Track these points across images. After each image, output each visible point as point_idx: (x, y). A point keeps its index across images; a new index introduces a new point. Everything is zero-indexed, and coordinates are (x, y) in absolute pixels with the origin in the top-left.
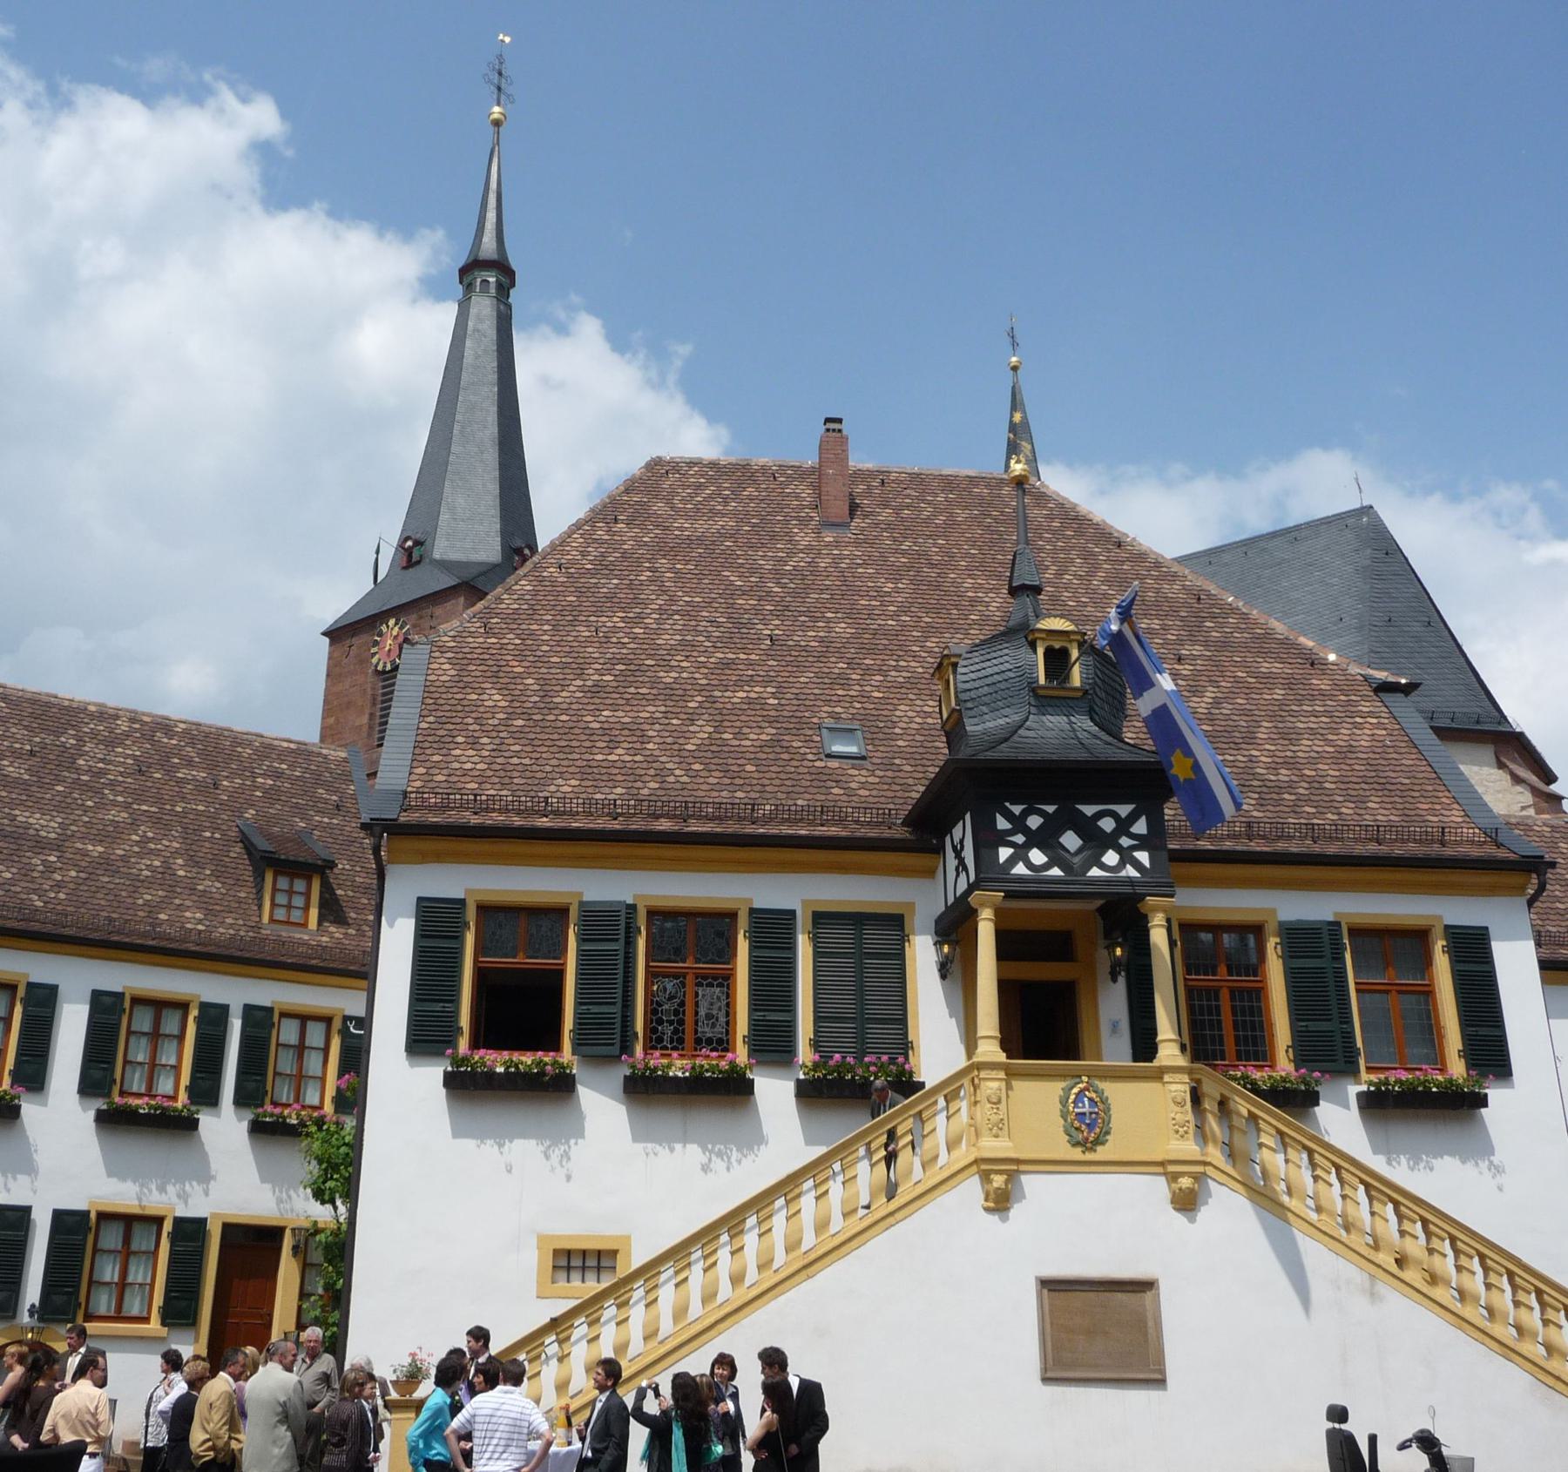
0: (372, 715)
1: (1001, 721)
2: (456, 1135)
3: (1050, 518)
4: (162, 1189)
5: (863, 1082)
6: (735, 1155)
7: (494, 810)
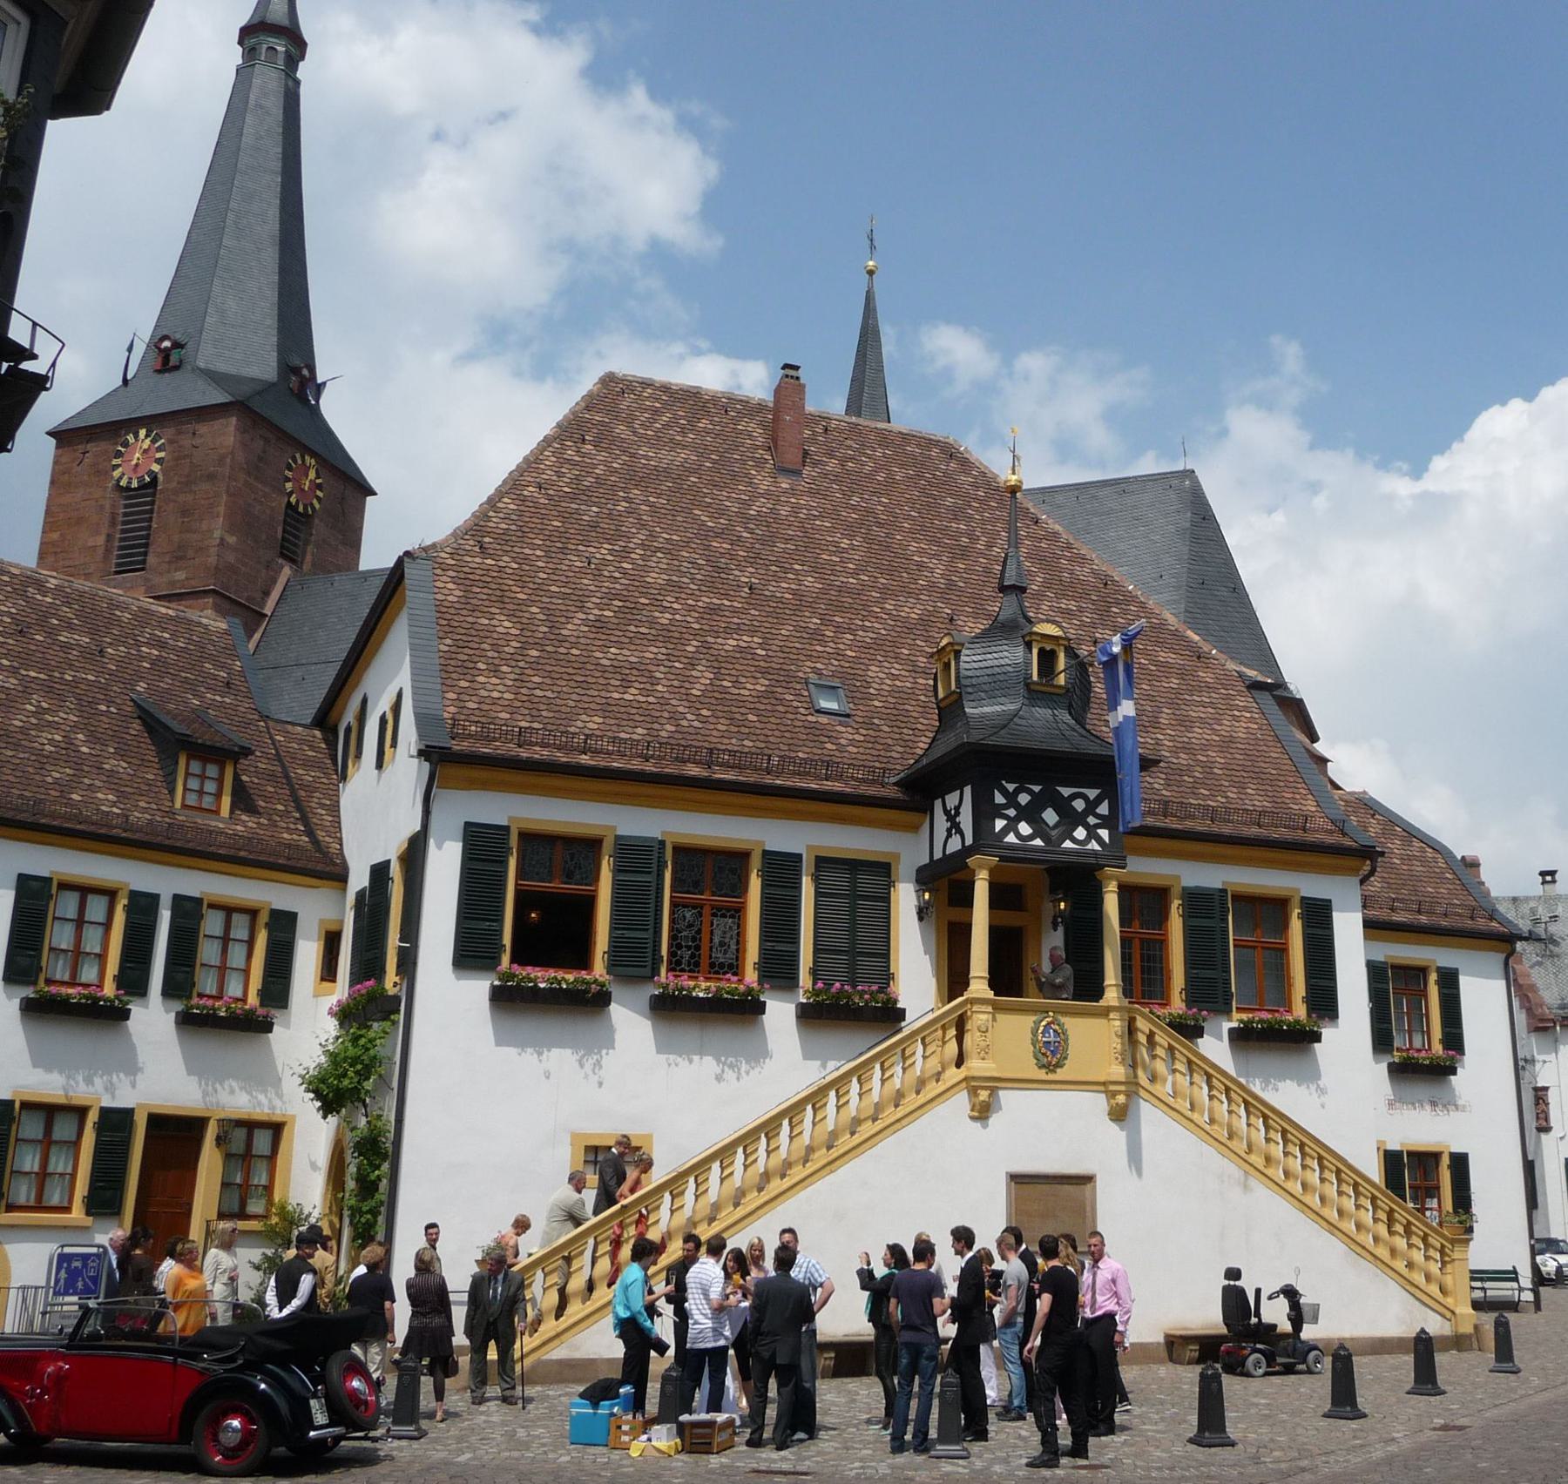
0: (109, 537)
1: (998, 708)
2: (498, 1043)
3: (976, 486)
4: (89, 1081)
5: (853, 1006)
6: (744, 1067)
7: (536, 744)
